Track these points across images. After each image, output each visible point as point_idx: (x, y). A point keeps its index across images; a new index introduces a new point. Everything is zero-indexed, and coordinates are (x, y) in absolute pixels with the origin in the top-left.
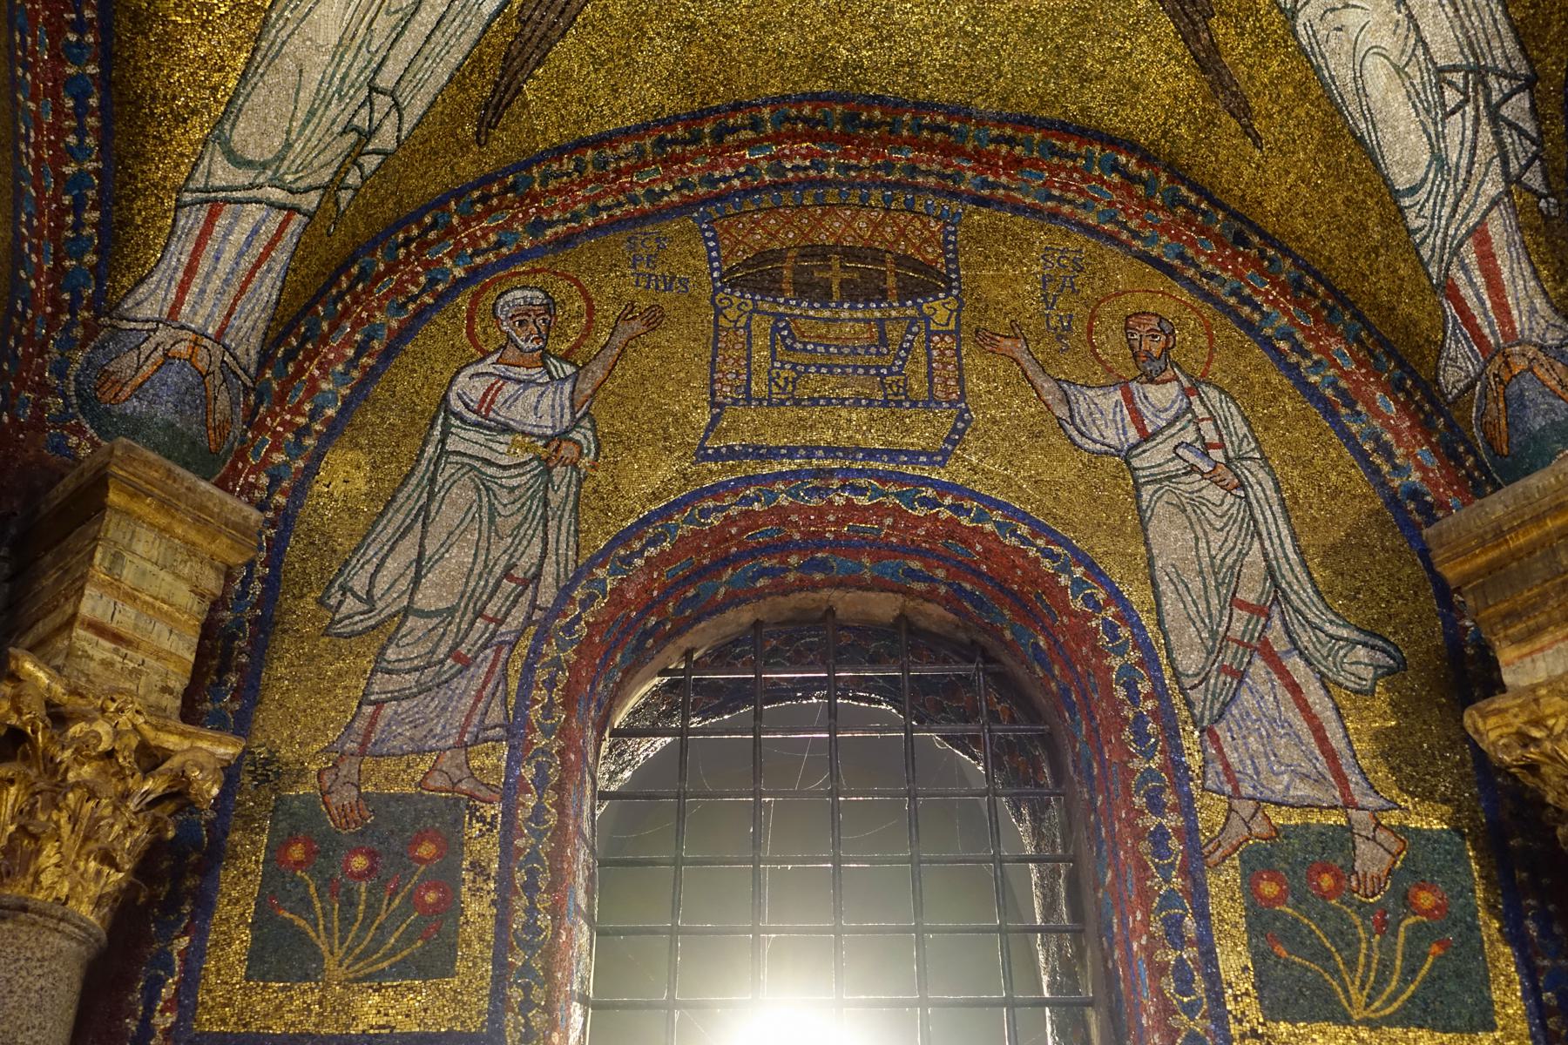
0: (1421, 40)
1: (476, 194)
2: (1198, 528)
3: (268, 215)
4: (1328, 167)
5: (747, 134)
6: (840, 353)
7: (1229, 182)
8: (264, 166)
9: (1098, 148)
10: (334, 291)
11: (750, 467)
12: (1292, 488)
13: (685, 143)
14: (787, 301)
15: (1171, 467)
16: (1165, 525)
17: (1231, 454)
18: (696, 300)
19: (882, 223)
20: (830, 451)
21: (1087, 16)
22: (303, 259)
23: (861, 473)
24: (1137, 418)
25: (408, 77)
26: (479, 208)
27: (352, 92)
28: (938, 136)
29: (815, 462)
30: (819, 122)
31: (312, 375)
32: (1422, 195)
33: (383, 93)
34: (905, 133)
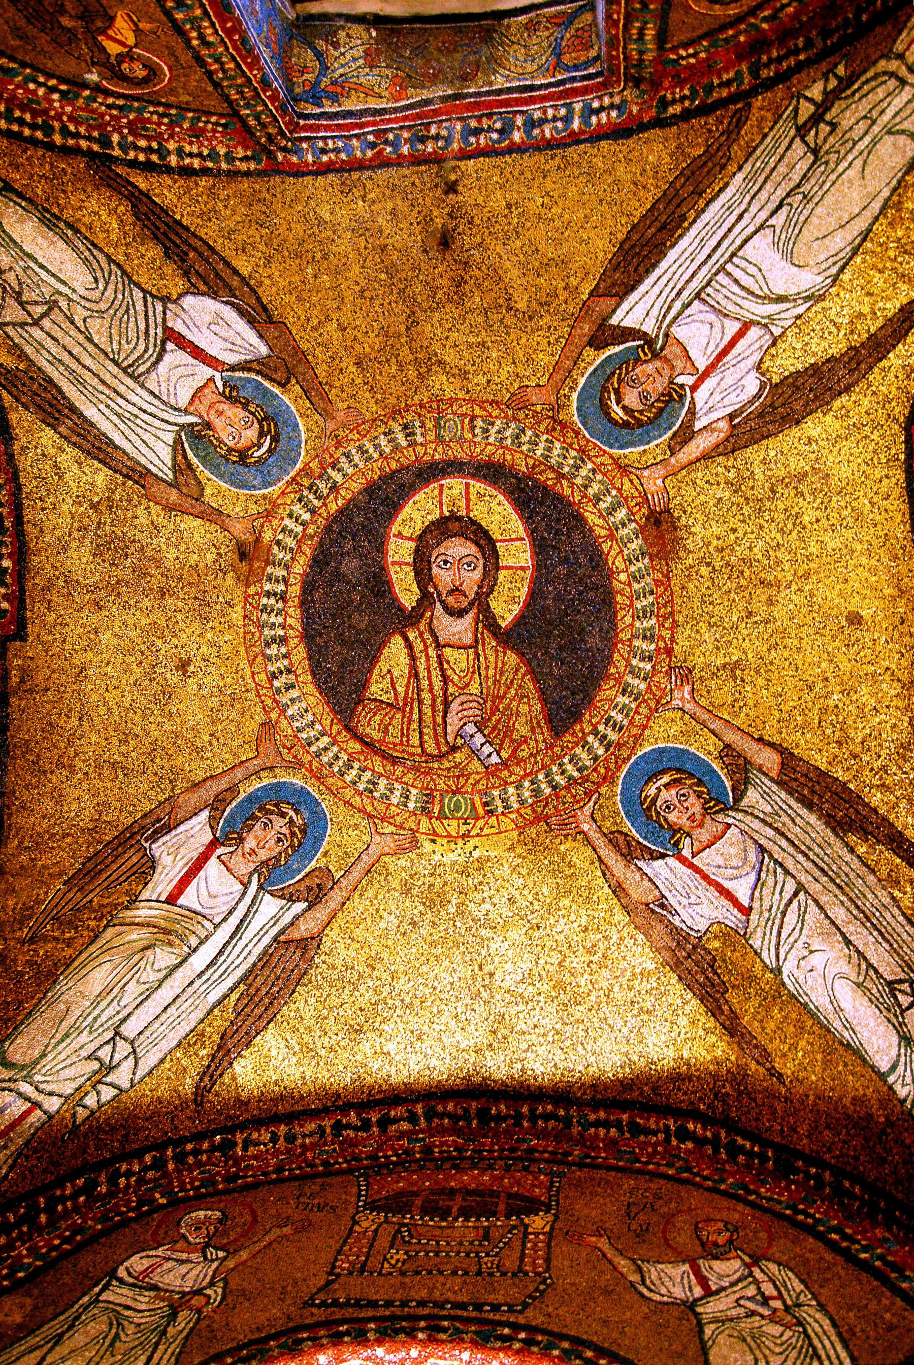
0: (870, 965)
1: (189, 1147)
2: (757, 1352)
3: (14, 1102)
4: (833, 1080)
5: (405, 1126)
6: (448, 1244)
7: (768, 1120)
8: (23, 1068)
9: (671, 1122)
10: (58, 1193)
11: (349, 1312)
12: (848, 1325)
13: (356, 1129)
14: (412, 1218)
15: (734, 1313)
16: (725, 1351)
17: (789, 1302)
18: (339, 1218)
19: (502, 1178)
20: (422, 1303)
21: (641, 1008)
22: (36, 1151)
23: (445, 1318)
24: (703, 1281)
25: (147, 1033)
26: (191, 1160)
27: (101, 1030)
28: (552, 1124)
29: (406, 1309)
30: (459, 1118)
31: (20, 1253)
32: (901, 1068)
33: (125, 1039)
34: (526, 1124)
